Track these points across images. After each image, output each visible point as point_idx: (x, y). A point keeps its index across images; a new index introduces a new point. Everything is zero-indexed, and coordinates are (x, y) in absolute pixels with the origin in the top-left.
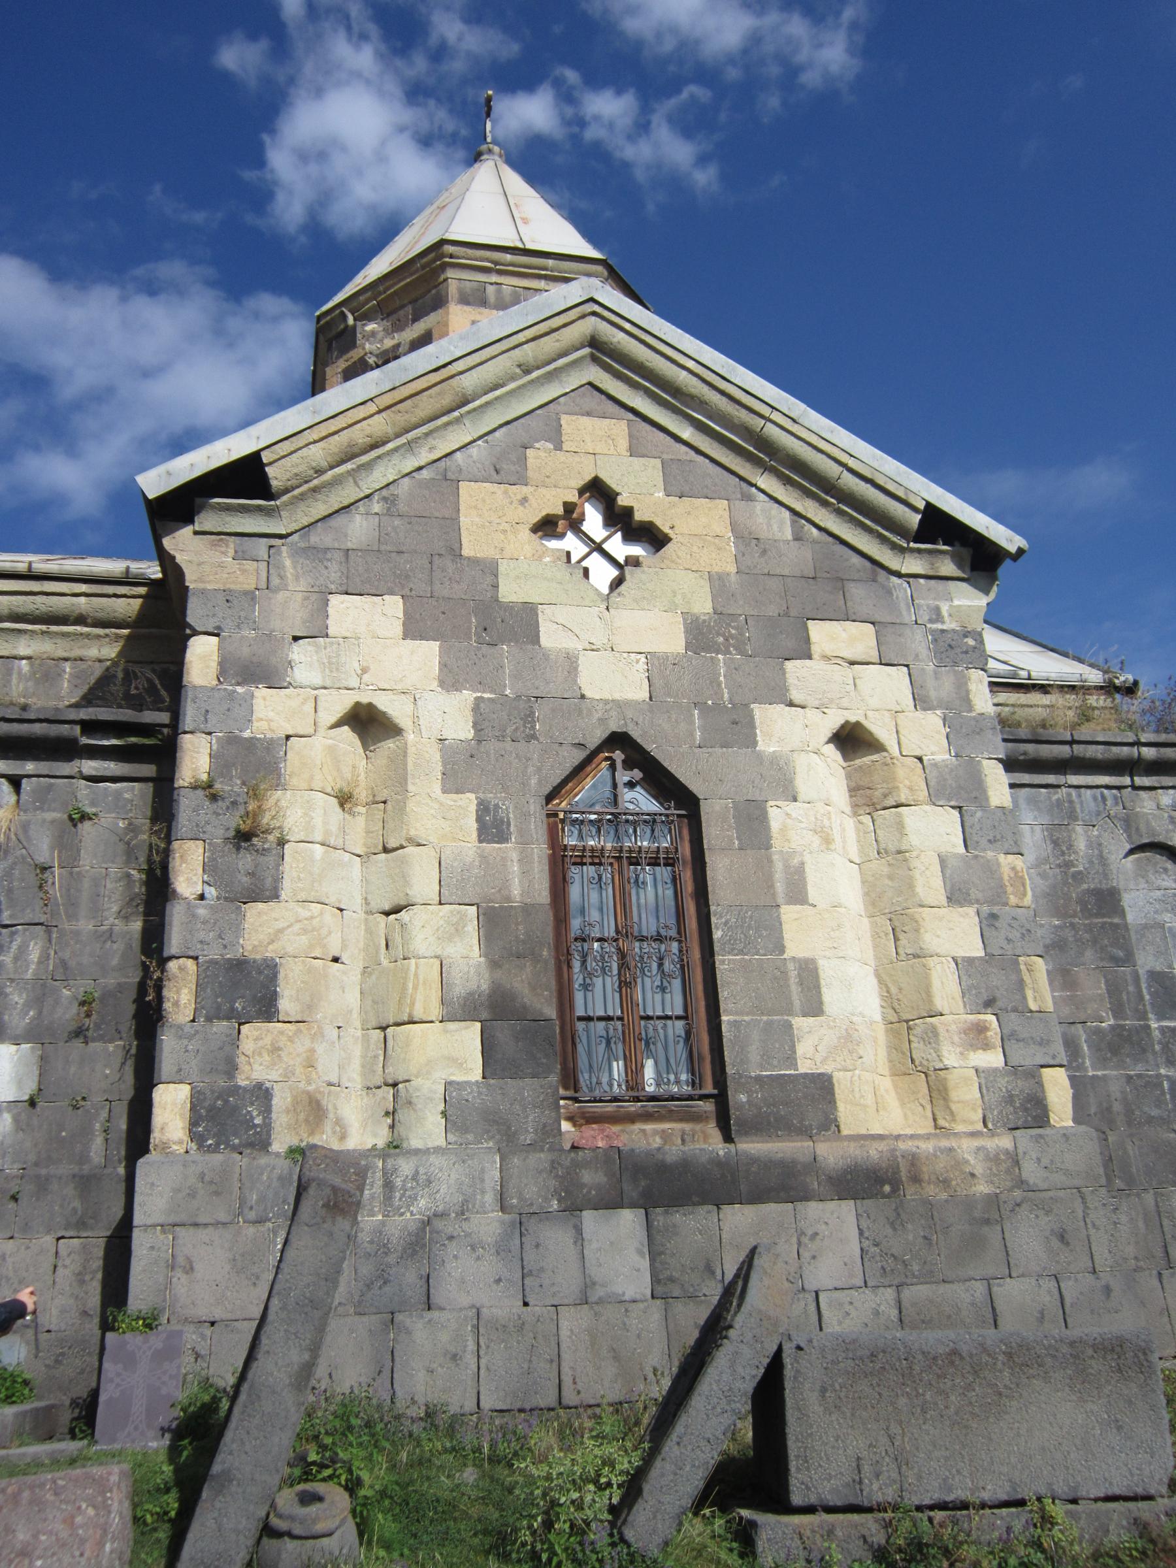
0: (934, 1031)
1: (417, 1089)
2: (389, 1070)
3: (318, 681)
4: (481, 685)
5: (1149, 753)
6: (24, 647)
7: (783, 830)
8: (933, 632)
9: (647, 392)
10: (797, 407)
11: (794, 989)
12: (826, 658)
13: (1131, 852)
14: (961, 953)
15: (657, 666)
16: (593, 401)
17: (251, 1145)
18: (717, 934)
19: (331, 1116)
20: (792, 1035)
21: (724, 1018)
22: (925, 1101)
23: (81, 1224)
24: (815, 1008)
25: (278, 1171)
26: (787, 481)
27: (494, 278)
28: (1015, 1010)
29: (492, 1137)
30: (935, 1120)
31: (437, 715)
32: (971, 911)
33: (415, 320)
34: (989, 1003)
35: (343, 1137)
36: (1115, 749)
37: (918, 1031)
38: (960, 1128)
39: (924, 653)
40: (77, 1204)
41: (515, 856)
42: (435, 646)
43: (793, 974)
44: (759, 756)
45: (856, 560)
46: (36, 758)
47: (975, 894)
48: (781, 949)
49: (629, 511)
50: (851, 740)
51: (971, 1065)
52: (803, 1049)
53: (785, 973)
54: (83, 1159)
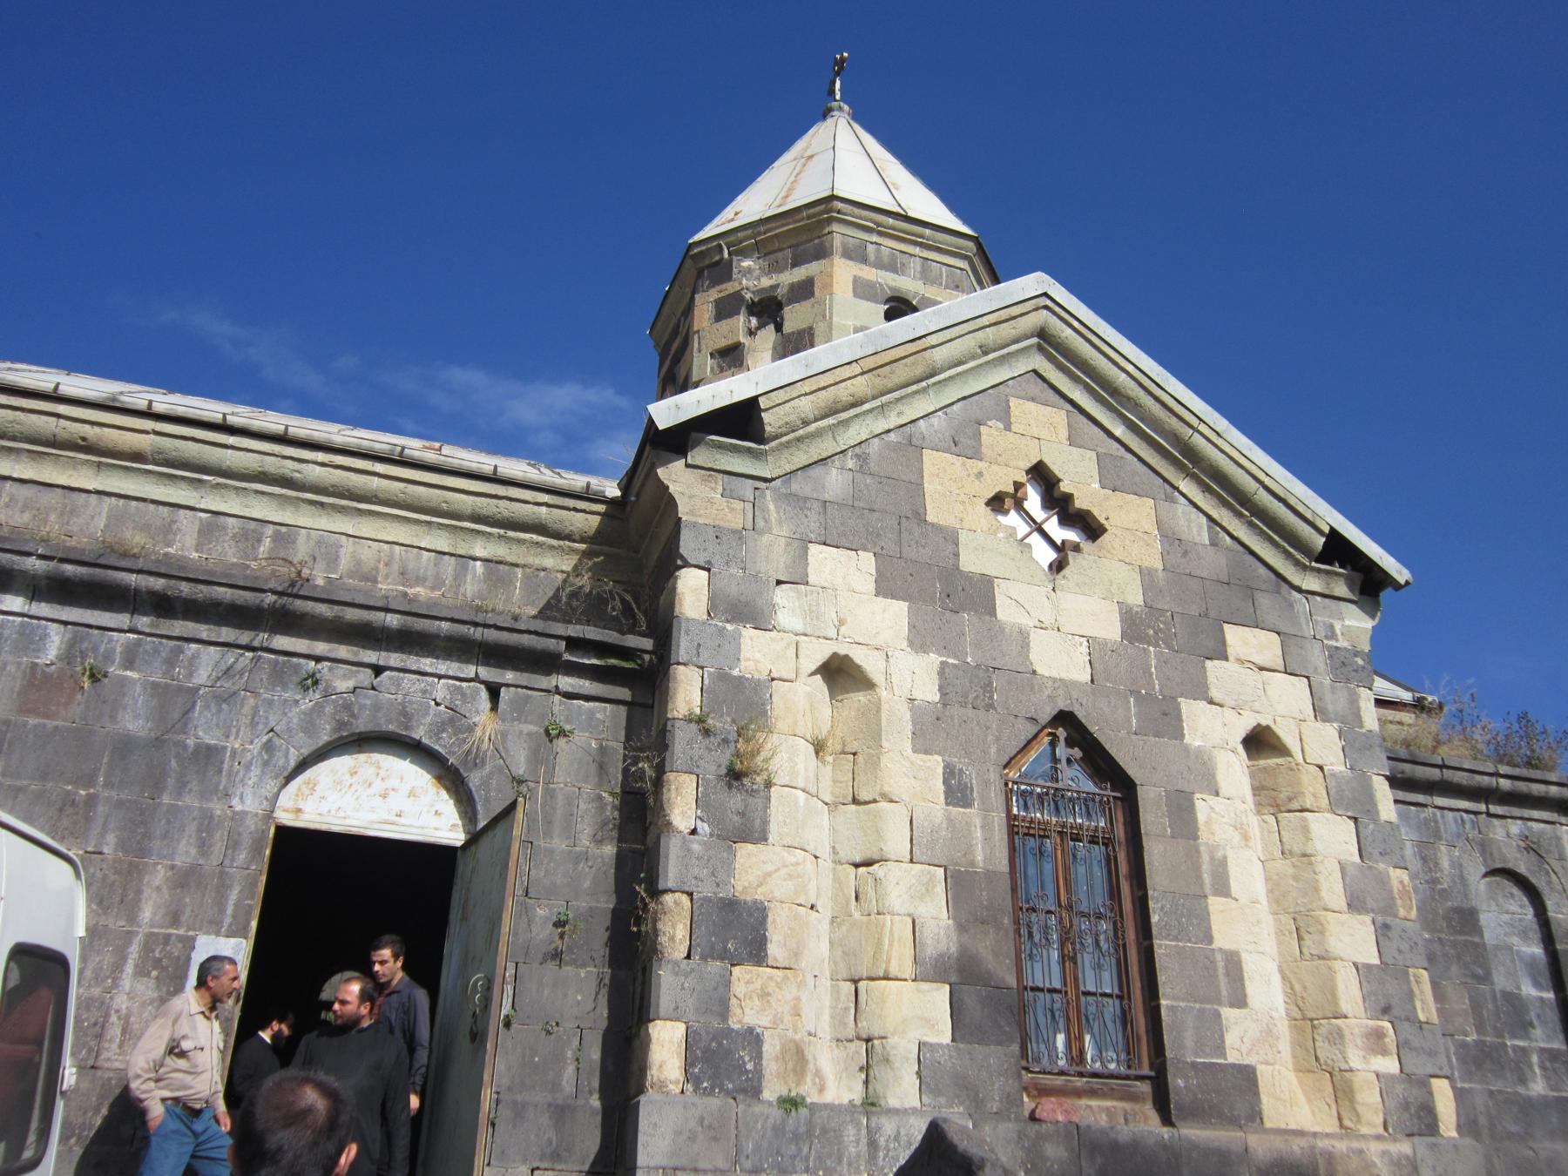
0: (1340, 1034)
1: (893, 1047)
2: (863, 1024)
3: (800, 627)
4: (945, 649)
5: (1505, 784)
6: (480, 549)
7: (1209, 822)
8: (1329, 648)
9: (1087, 387)
10: (1222, 424)
11: (1222, 979)
12: (1241, 661)
13: (1486, 875)
14: (1361, 959)
15: (1097, 651)
16: (1038, 388)
17: (744, 1091)
18: (1155, 919)
19: (811, 1066)
20: (1220, 1024)
21: (1163, 1002)
22: (1331, 1100)
23: (556, 1156)
24: (1240, 1001)
25: (771, 1121)
26: (1207, 489)
27: (875, 238)
28: (1408, 1019)
29: (961, 1103)
30: (1340, 1119)
31: (908, 676)
32: (1367, 919)
33: (794, 265)
34: (1386, 1010)
35: (822, 1090)
36: (1478, 778)
37: (1323, 1031)
38: (1364, 1130)
39: (1322, 667)
40: (551, 1134)
41: (978, 822)
42: (904, 605)
43: (1221, 965)
44: (1186, 748)
45: (1262, 570)
46: (515, 668)
47: (1370, 903)
48: (1209, 938)
49: (1068, 498)
50: (1259, 742)
51: (1371, 1068)
52: (1231, 1039)
53: (1213, 962)
54: (555, 1087)
